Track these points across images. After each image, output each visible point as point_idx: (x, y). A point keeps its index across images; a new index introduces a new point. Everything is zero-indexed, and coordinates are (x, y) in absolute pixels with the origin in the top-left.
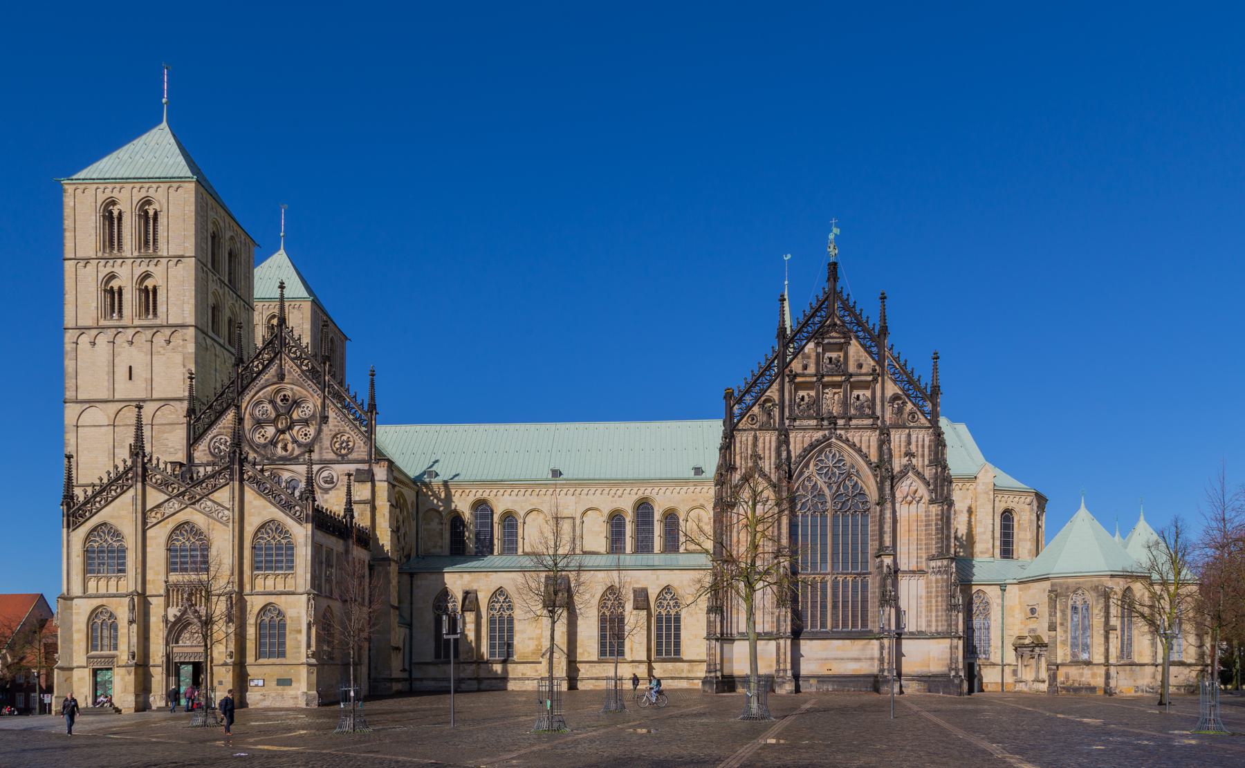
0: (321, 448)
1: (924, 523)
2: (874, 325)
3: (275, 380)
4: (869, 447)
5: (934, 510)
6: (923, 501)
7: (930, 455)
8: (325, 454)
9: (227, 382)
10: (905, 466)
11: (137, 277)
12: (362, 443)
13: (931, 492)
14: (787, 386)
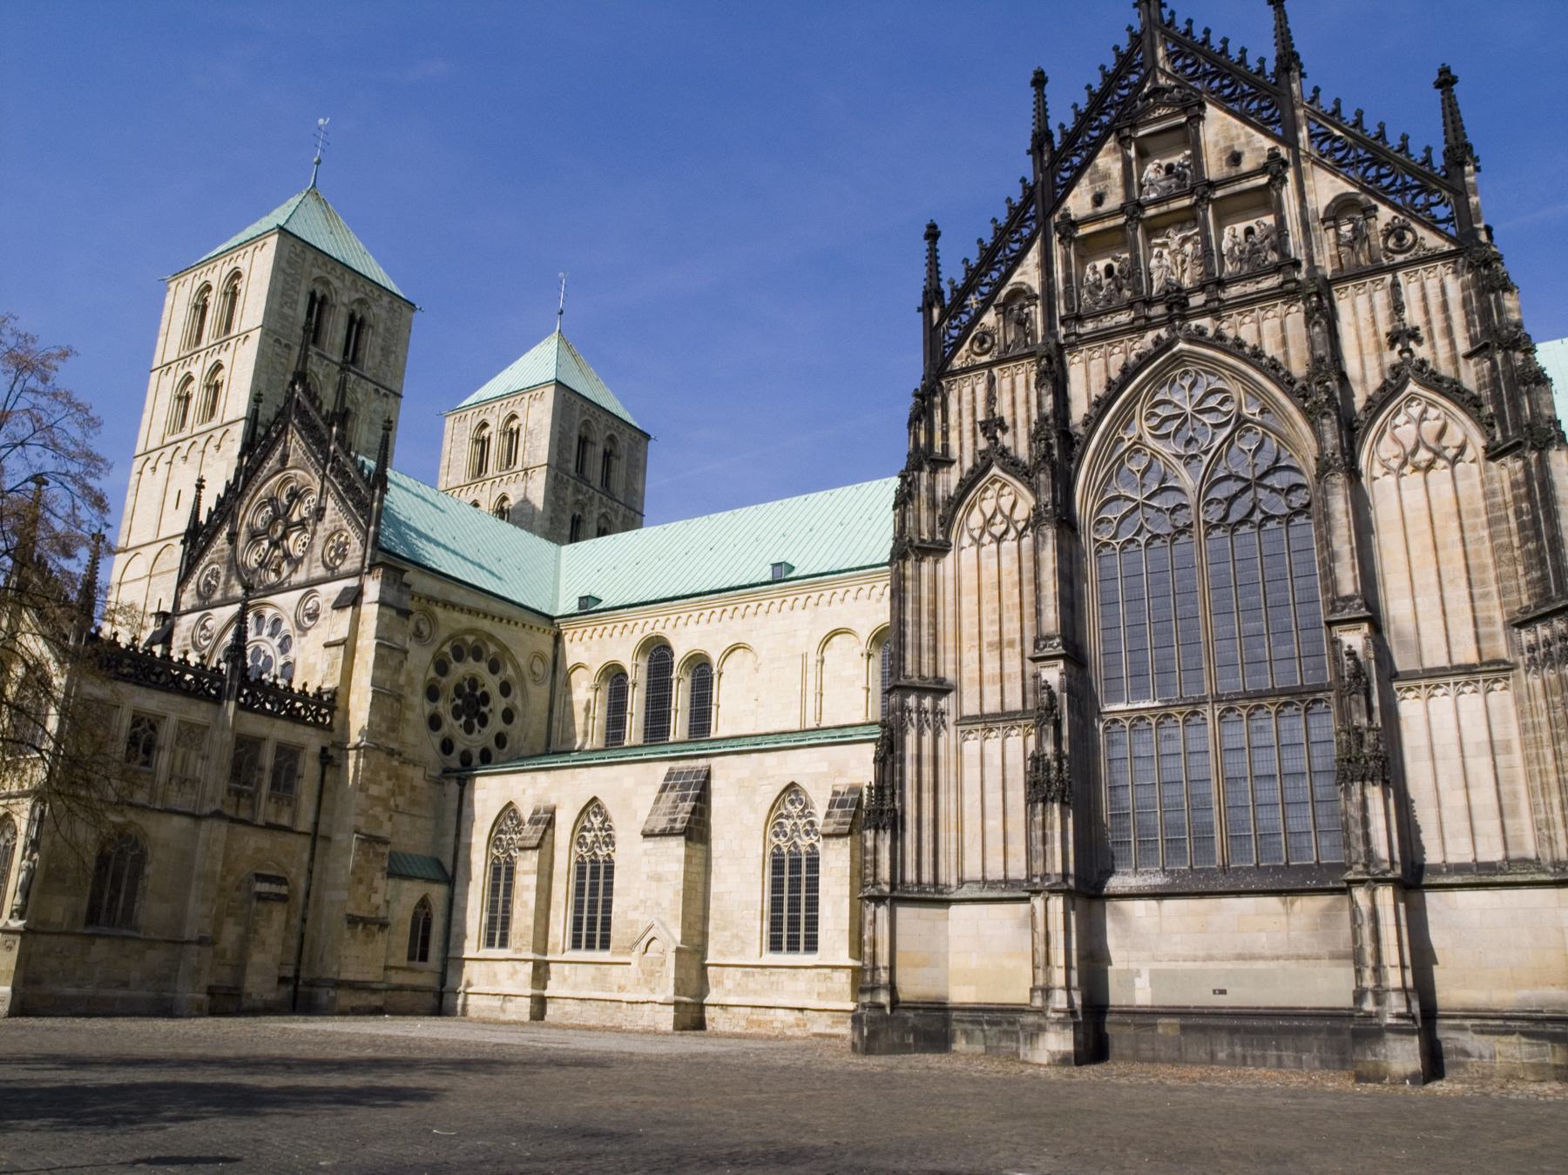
0: (310, 562)
1: (1484, 518)
2: (1262, 61)
3: (278, 466)
4: (1284, 342)
5: (1505, 473)
6: (1470, 453)
7: (1469, 324)
8: (313, 570)
10: (1393, 367)
13: (1486, 425)
14: (1058, 251)
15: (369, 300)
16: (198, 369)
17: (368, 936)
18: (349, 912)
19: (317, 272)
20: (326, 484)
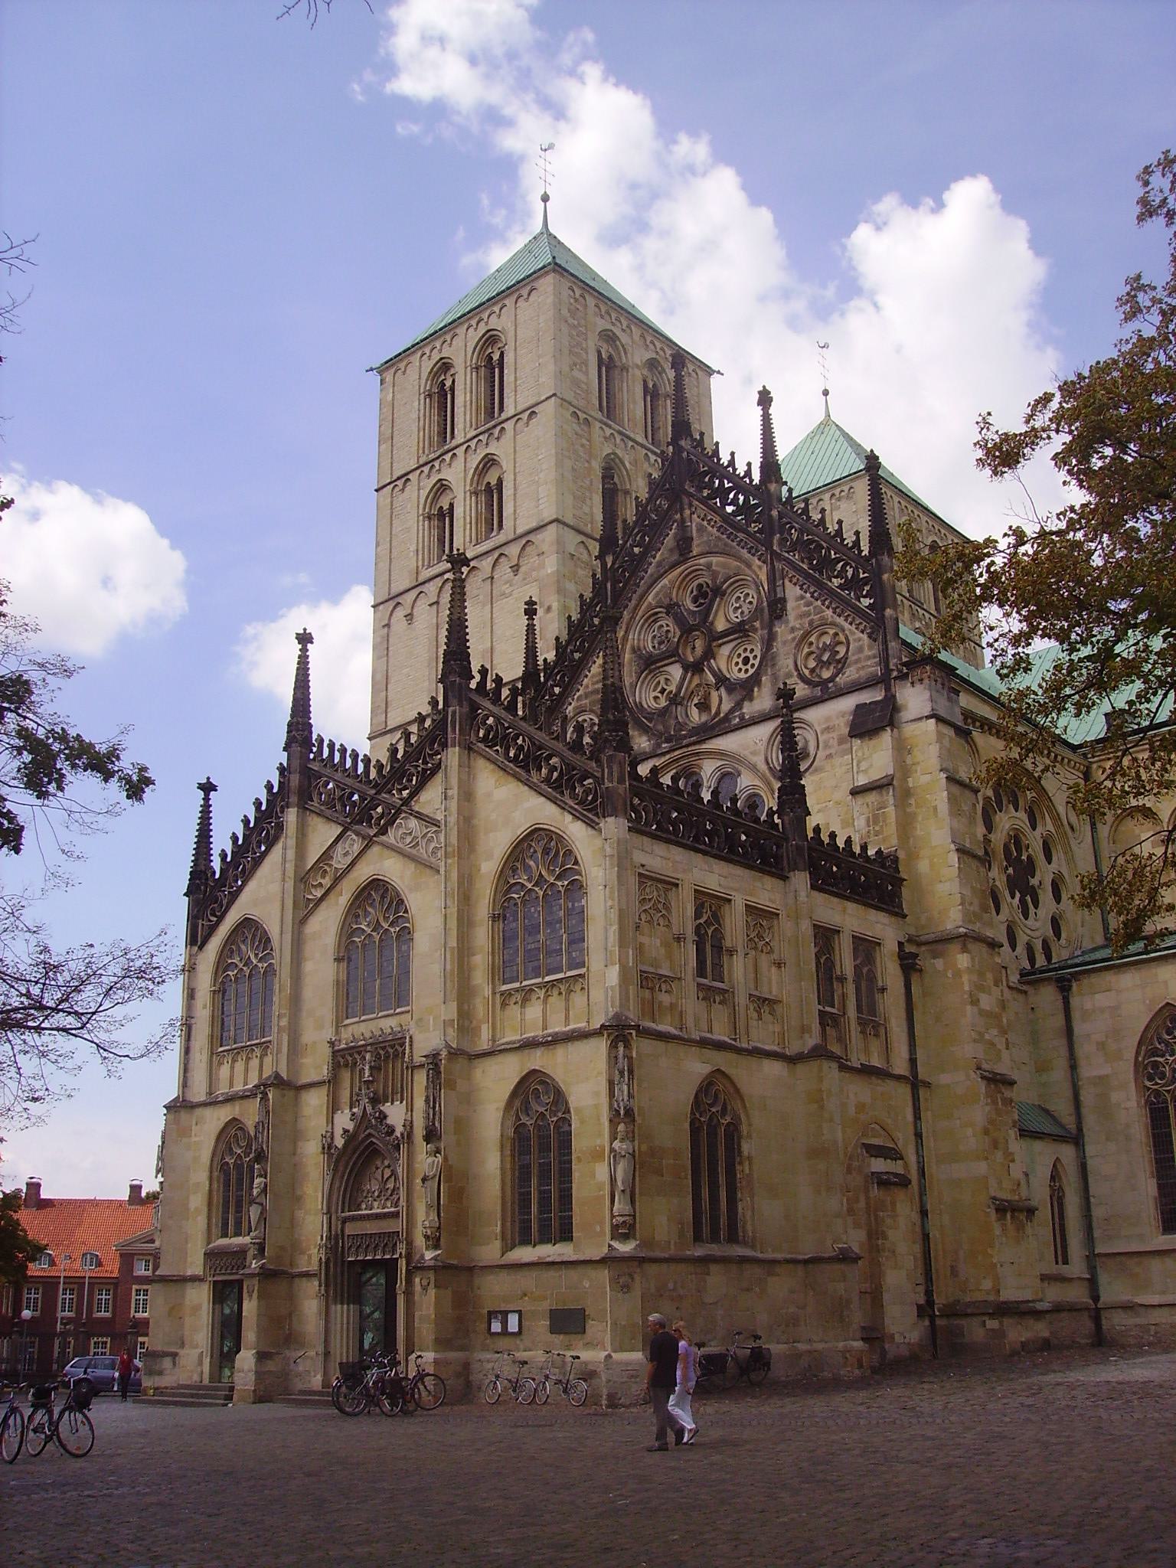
3: (675, 557)
9: (588, 595)
11: (472, 471)
12: (865, 637)
15: (661, 361)
16: (458, 473)
17: (1018, 1230)
18: (993, 1194)
19: (602, 324)
20: (778, 565)
